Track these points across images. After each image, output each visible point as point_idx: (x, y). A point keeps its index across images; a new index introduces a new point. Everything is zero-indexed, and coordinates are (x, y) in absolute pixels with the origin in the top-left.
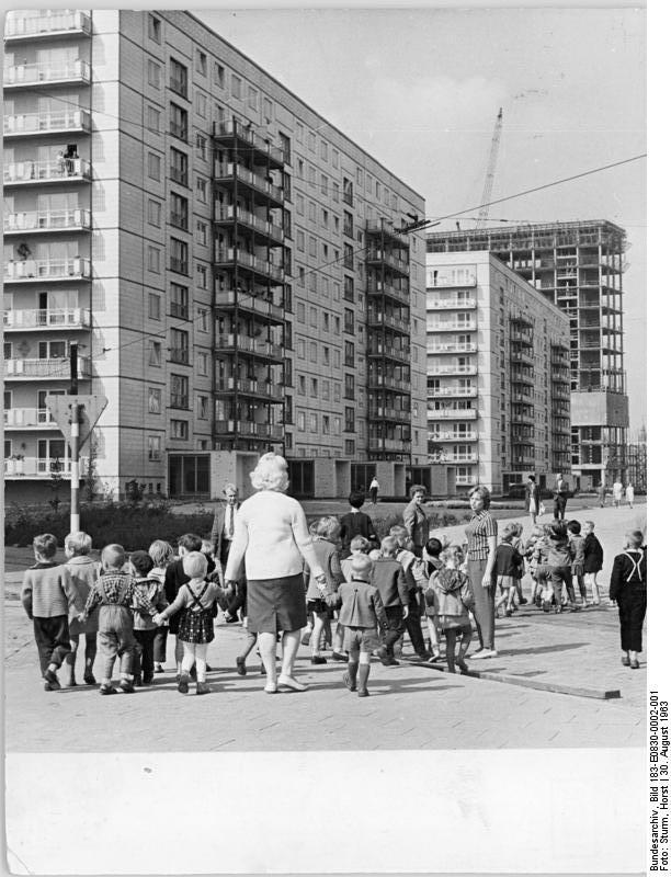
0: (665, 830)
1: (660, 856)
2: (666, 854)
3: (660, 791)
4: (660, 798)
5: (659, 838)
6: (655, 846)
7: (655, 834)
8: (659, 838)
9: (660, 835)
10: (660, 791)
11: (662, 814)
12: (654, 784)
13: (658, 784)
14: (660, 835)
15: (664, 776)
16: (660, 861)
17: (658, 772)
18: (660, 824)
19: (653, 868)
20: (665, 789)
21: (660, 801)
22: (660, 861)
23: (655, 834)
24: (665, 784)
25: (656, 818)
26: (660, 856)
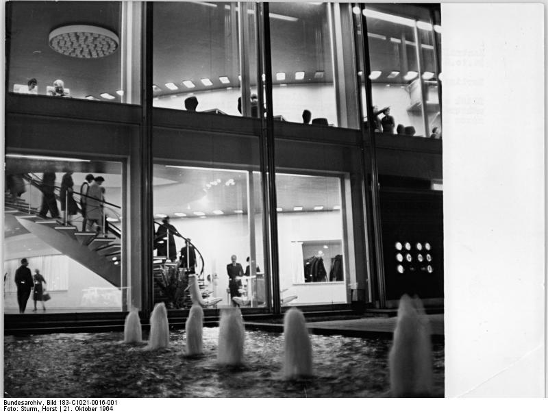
0: (30, 409)
1: (13, 406)
2: (15, 409)
3: (54, 406)
4: (50, 406)
5: (24, 405)
6: (19, 403)
7: (27, 403)
8: (24, 405)
9: (27, 406)
10: (54, 406)
11: (39, 407)
12: (58, 403)
13: (58, 405)
14: (27, 406)
15: (63, 409)
16: (10, 406)
17: (65, 405)
18: (33, 406)
19: (5, 402)
20: (55, 409)
21: (48, 406)
22: (10, 406)
23: (27, 403)
24: (58, 409)
25: (37, 403)
26: (13, 406)
